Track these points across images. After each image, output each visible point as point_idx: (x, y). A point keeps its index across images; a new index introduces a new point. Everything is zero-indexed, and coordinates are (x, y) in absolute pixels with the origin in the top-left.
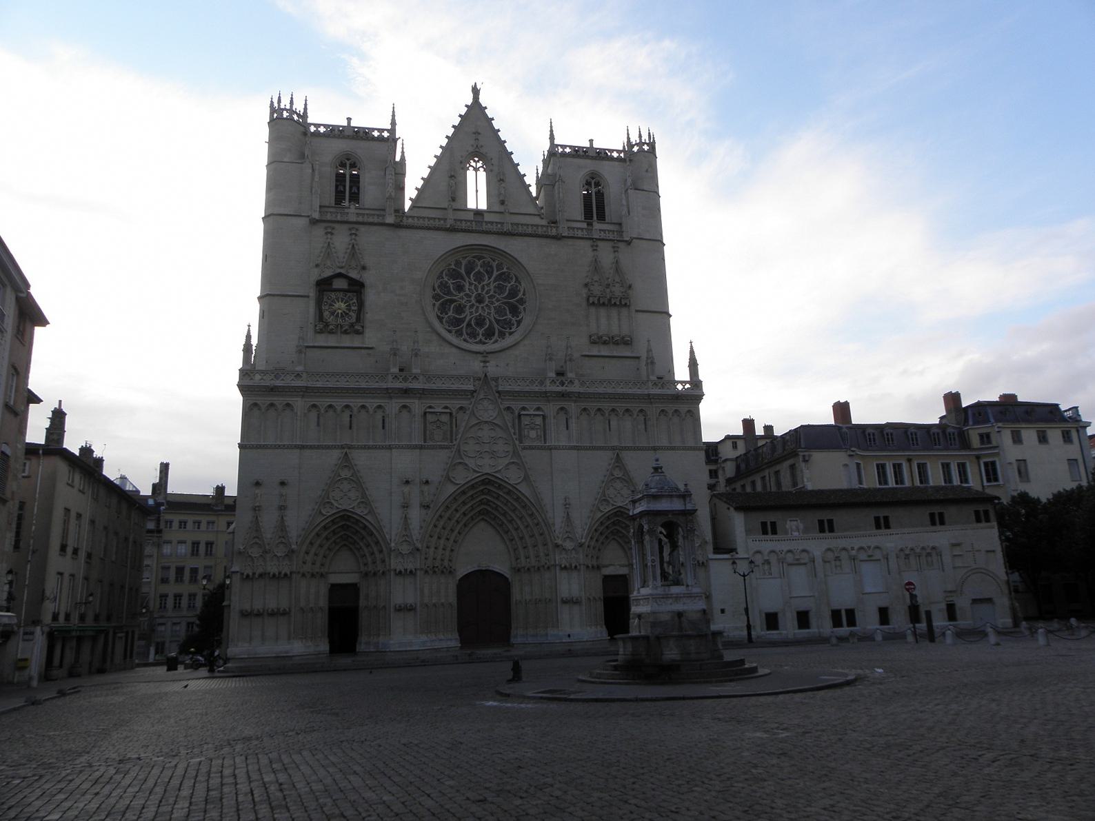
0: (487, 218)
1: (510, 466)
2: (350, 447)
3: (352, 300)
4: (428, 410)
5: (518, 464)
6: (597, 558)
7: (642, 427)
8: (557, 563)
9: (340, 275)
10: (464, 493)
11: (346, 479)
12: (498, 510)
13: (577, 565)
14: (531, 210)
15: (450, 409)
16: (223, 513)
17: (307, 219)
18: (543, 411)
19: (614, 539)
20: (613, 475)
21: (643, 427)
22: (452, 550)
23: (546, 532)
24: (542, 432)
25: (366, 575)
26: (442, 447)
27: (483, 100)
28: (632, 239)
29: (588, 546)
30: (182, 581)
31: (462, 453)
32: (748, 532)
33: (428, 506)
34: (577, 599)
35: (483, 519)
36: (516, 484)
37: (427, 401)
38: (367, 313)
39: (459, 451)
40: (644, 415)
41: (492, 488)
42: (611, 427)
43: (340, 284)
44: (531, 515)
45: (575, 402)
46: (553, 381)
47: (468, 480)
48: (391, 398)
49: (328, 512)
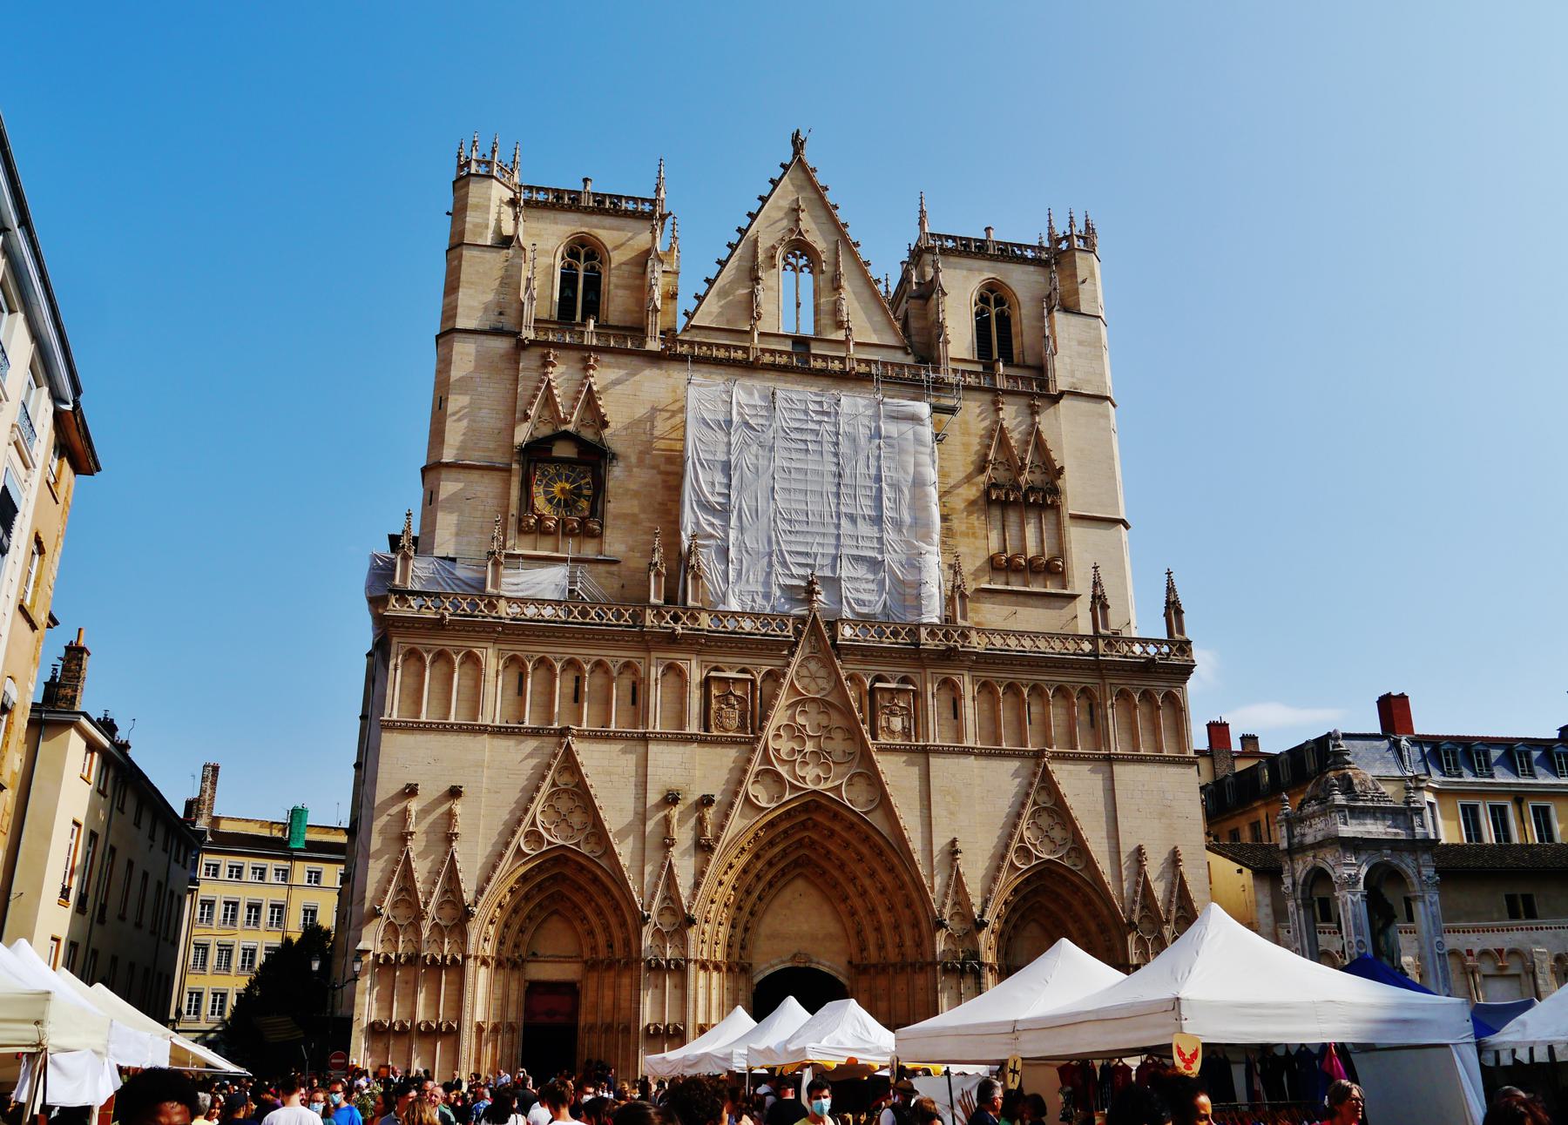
3: (585, 478)
4: (713, 674)
7: (1082, 717)
9: (566, 436)
11: (565, 791)
15: (752, 675)
16: (303, 854)
17: (513, 341)
21: (1088, 717)
23: (918, 903)
24: (912, 721)
25: (592, 966)
26: (733, 742)
27: (808, 156)
28: (1062, 394)
30: (228, 964)
35: (799, 875)
36: (865, 813)
37: (712, 659)
39: (766, 749)
40: (1088, 698)
43: (563, 450)
44: (891, 870)
45: (970, 669)
46: (932, 634)
48: (648, 650)
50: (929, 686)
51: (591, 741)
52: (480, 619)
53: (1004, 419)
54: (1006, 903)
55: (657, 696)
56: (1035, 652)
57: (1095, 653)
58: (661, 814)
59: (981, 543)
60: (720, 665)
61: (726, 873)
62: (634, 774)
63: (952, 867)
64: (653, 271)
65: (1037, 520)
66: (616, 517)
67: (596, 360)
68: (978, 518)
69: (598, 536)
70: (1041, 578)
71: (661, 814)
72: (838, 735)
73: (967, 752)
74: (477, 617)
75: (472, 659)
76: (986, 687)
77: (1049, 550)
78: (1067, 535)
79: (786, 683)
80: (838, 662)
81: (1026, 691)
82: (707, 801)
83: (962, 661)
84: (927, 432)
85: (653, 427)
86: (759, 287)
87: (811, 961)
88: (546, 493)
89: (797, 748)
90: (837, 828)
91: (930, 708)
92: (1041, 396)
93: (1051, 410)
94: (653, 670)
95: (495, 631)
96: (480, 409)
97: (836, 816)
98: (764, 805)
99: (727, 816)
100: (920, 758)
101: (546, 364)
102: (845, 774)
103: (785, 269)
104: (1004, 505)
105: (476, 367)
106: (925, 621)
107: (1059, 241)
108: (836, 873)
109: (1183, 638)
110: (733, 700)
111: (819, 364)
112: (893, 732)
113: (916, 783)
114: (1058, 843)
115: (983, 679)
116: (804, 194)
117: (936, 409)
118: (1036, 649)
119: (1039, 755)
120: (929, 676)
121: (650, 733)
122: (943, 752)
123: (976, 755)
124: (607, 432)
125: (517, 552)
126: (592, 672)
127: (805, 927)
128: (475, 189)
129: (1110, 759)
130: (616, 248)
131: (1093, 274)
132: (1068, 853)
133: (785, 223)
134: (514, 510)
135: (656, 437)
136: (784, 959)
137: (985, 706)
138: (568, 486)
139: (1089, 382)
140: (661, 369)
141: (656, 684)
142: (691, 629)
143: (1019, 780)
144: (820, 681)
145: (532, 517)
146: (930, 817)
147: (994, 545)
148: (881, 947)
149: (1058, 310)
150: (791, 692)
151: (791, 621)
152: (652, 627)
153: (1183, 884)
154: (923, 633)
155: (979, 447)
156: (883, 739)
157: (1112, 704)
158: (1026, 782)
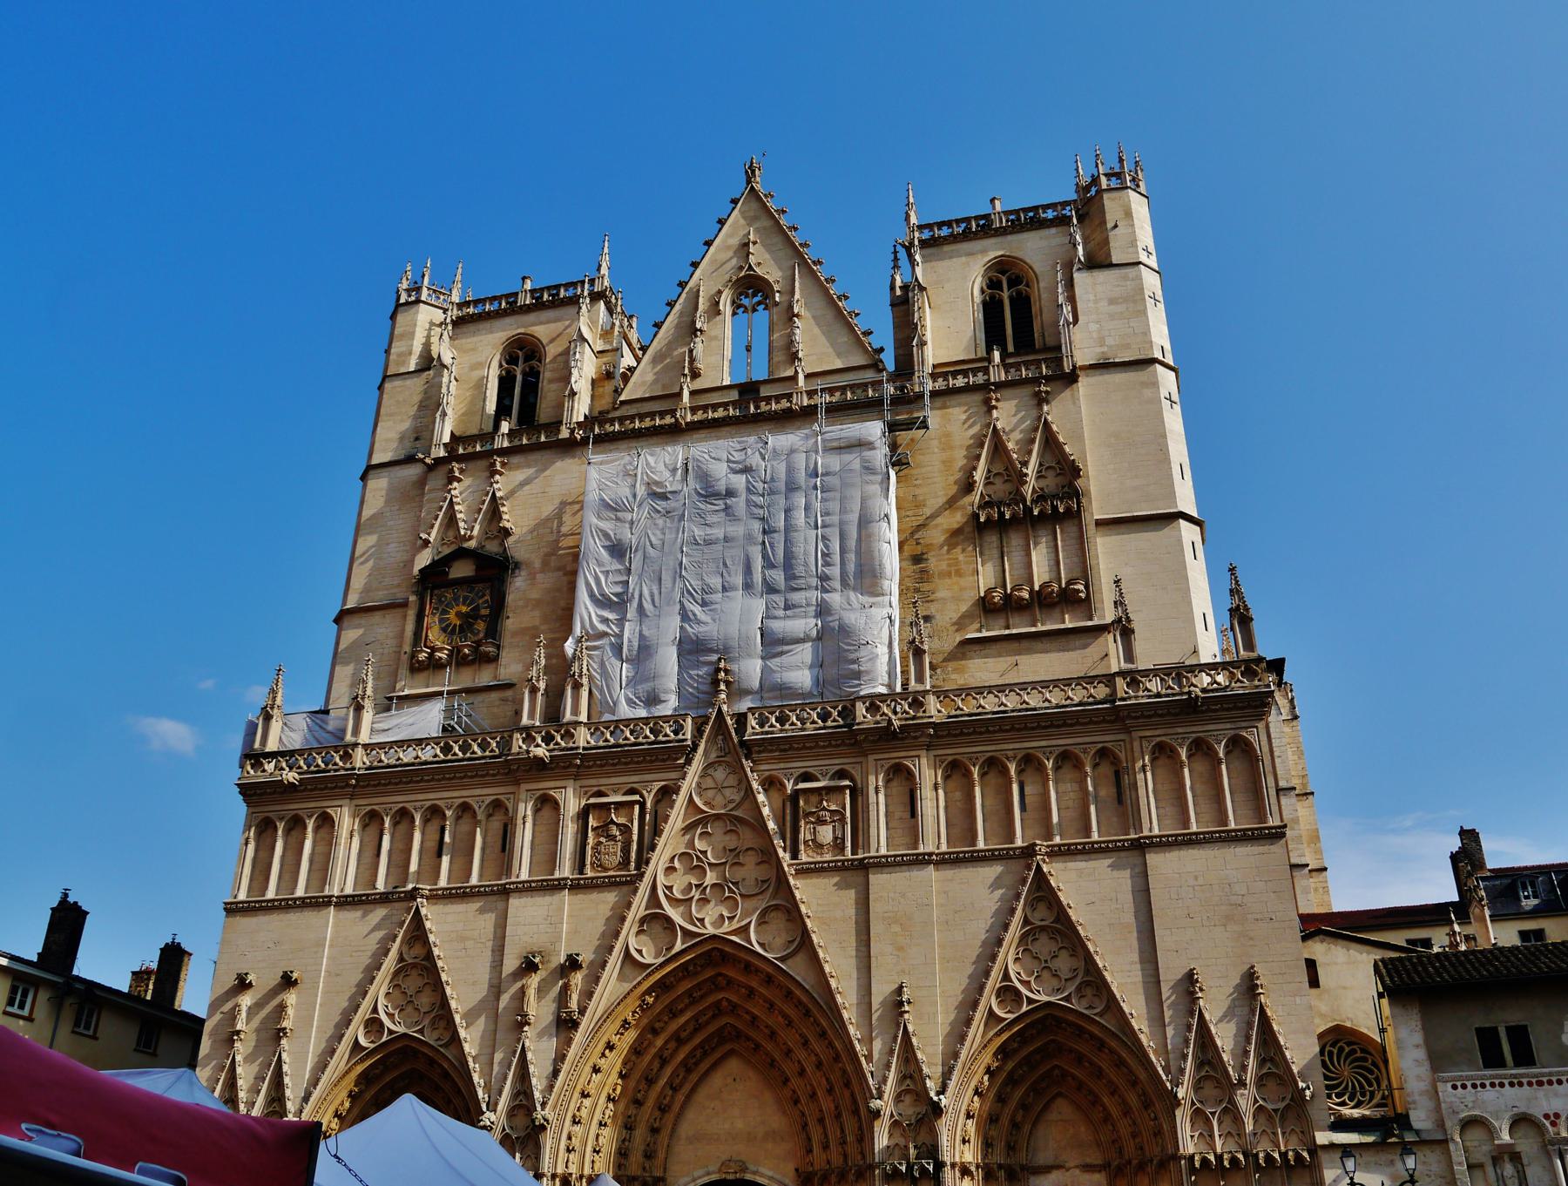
0: (765, 391)
1: (772, 914)
3: (484, 595)
6: (1011, 1148)
7: (1107, 792)
14: (858, 359)
18: (852, 779)
19: (1059, 1095)
26: (612, 884)
32: (1438, 1060)
35: (731, 1053)
36: (782, 959)
38: (508, 617)
40: (1112, 763)
41: (731, 973)
42: (1027, 800)
43: (461, 570)
45: (929, 748)
46: (873, 708)
48: (517, 783)
50: (872, 779)
51: (447, 901)
52: (332, 773)
53: (997, 419)
54: (988, 1071)
55: (525, 835)
56: (1020, 711)
57: (1111, 699)
58: (519, 985)
59: (967, 581)
60: (602, 788)
61: (603, 1055)
62: (492, 937)
64: (575, 353)
65: (1050, 537)
66: (515, 634)
67: (503, 464)
68: (963, 550)
69: (493, 660)
70: (1057, 610)
71: (519, 985)
72: (750, 860)
73: (922, 861)
74: (329, 771)
75: (326, 822)
76: (955, 770)
77: (1066, 574)
78: (1093, 548)
79: (680, 800)
80: (747, 764)
81: (1012, 768)
82: (573, 964)
83: (916, 738)
84: (880, 454)
85: (560, 524)
86: (698, 340)
87: (744, 1169)
88: (441, 621)
89: (694, 882)
90: (754, 984)
91: (872, 808)
92: (1049, 379)
93: (1067, 393)
94: (521, 806)
95: (348, 785)
96: (388, 544)
98: (648, 960)
99: (597, 979)
100: (857, 877)
101: (451, 479)
102: (754, 912)
103: (734, 314)
104: (1001, 526)
105: (387, 502)
106: (862, 693)
107: (1087, 188)
108: (769, 1047)
109: (1253, 655)
110: (615, 831)
111: (764, 407)
112: (821, 846)
113: (852, 912)
114: (1063, 977)
115: (950, 758)
116: (755, 226)
117: (893, 427)
118: (1024, 706)
119: (1029, 852)
120: (872, 769)
122: (888, 865)
123: (937, 864)
124: (511, 540)
125: (406, 692)
126: (458, 818)
127: (739, 1124)
128: (401, 318)
129: (1141, 847)
130: (552, 341)
131: (1128, 214)
132: (1079, 989)
133: (734, 262)
134: (407, 648)
135: (564, 535)
136: (711, 1169)
137: (958, 795)
138: (464, 609)
139: (1127, 346)
140: (574, 457)
141: (524, 823)
142: (563, 750)
143: (1001, 891)
144: (727, 792)
145: (422, 651)
146: (869, 956)
147: (986, 578)
148: (826, 1147)
149: (1079, 269)
150: (691, 810)
151: (689, 720)
152: (518, 754)
153: (1265, 1022)
154: (861, 709)
155: (965, 461)
156: (804, 857)
157: (1144, 766)
158: (1012, 893)
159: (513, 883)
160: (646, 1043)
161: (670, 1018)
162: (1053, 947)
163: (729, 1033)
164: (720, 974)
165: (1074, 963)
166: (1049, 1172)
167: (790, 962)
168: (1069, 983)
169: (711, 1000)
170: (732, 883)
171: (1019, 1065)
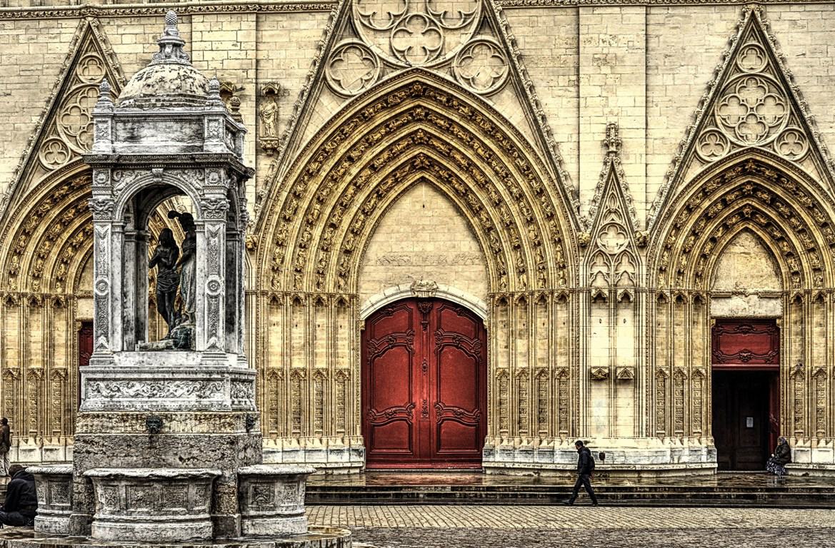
2: (98, 14)
5: (495, 47)
8: (581, 285)
10: (362, 117)
12: (454, 160)
13: (632, 292)
20: (738, 69)
22: (348, 252)
29: (667, 248)
31: (357, 23)
33: (274, 150)
34: (626, 372)
35: (423, 180)
36: (489, 95)
47: (369, 87)
49: (56, 163)
63: (605, 163)
90: (455, 118)
97: (450, 102)
121: (192, 6)
127: (430, 248)
132: (780, 137)
136: (403, 288)
148: (522, 271)
159: (196, 5)
160: (342, 170)
161: (366, 148)
162: (760, 95)
163: (422, 162)
164: (419, 106)
165: (779, 112)
166: (730, 297)
167: (494, 98)
168: (772, 131)
169: (405, 132)
170: (432, 14)
171: (715, 203)
